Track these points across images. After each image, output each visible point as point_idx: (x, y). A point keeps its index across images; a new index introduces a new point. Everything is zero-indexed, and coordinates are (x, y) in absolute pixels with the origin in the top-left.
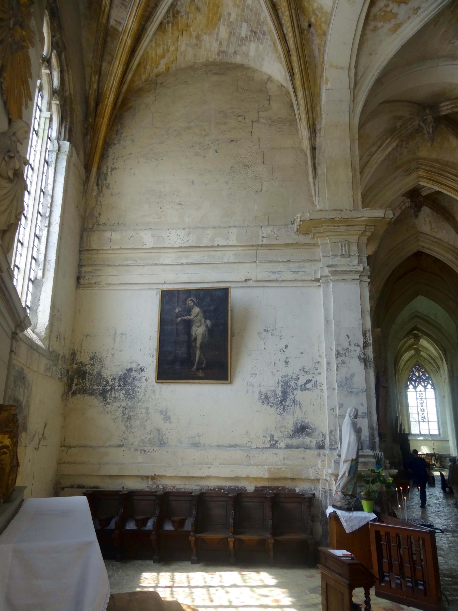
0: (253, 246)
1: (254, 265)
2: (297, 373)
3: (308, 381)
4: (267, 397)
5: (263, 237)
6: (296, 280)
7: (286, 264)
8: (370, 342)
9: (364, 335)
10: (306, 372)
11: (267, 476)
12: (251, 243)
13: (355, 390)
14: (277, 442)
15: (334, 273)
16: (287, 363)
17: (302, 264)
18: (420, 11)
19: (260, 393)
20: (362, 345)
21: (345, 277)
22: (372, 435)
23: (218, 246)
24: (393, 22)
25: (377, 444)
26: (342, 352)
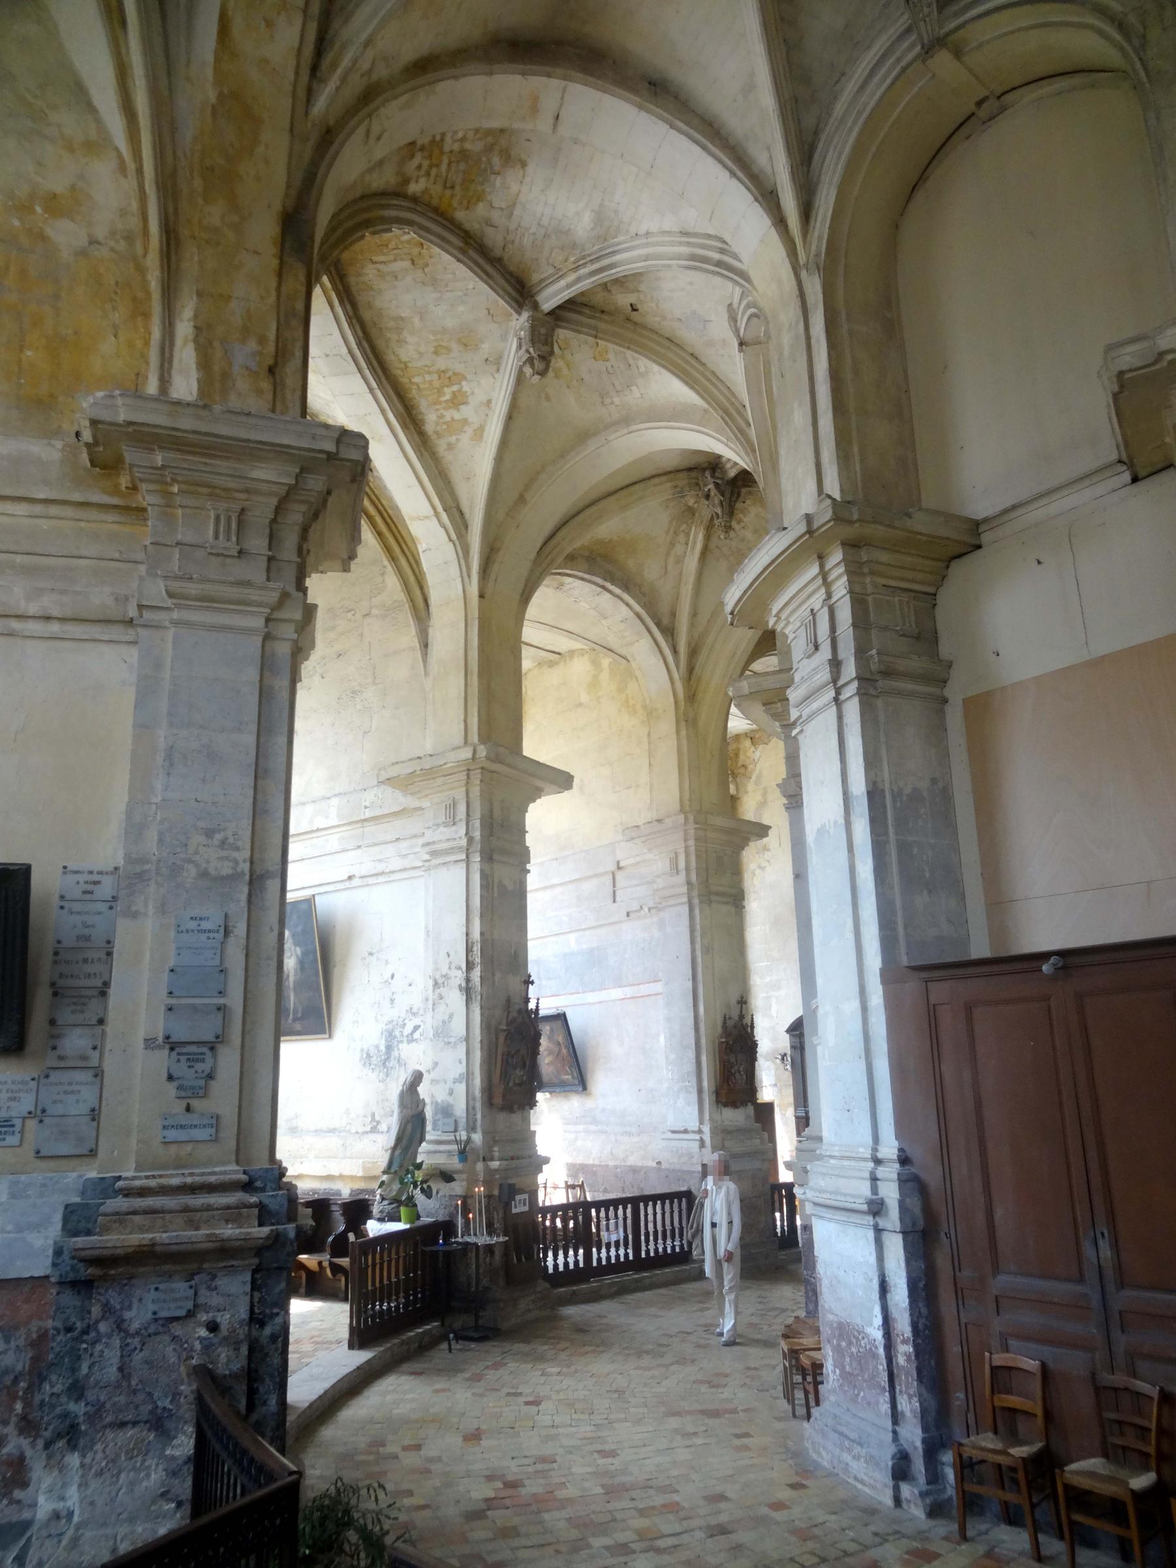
0: (357, 822)
1: (359, 851)
2: (403, 1015)
3: (416, 1028)
4: (369, 1056)
5: (366, 807)
6: (405, 869)
7: (396, 844)
8: (478, 960)
9: (469, 950)
10: (414, 1014)
11: (360, 1174)
12: (354, 819)
13: (452, 1040)
14: (378, 1122)
15: (434, 854)
16: (392, 1001)
17: (414, 840)
18: (493, 404)
19: (362, 1050)
20: (464, 968)
21: (448, 859)
22: (470, 1109)
23: (318, 830)
24: (469, 431)
25: (479, 1123)
26: (440, 981)
